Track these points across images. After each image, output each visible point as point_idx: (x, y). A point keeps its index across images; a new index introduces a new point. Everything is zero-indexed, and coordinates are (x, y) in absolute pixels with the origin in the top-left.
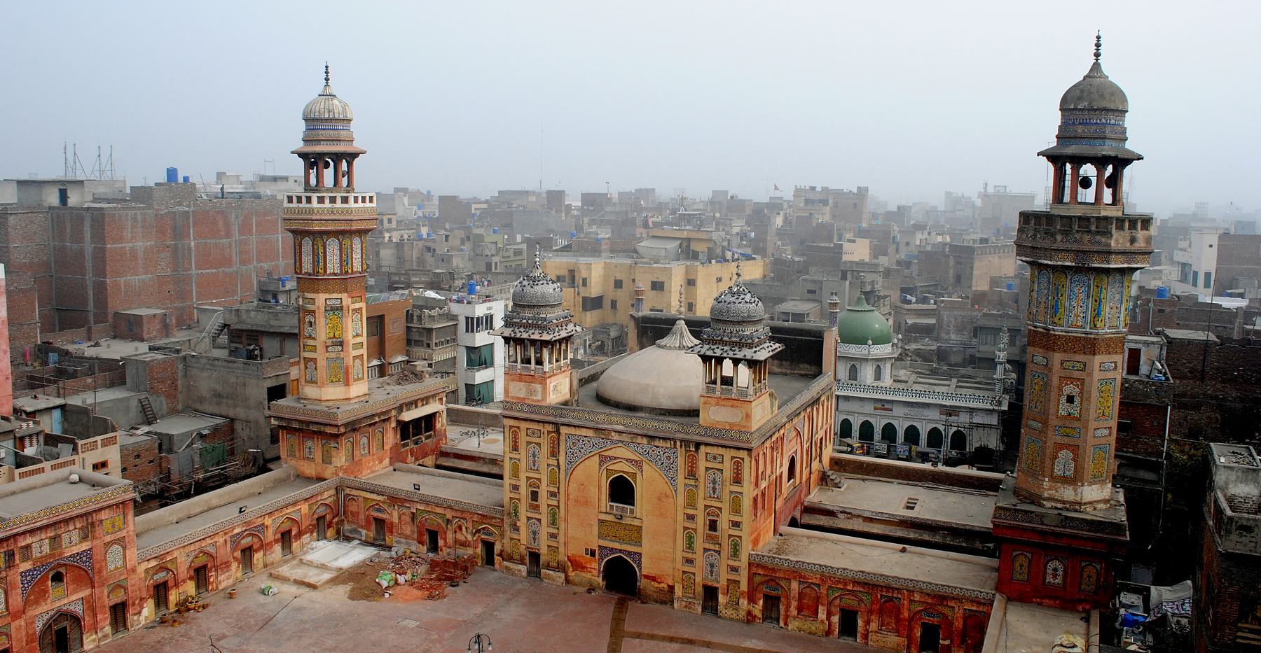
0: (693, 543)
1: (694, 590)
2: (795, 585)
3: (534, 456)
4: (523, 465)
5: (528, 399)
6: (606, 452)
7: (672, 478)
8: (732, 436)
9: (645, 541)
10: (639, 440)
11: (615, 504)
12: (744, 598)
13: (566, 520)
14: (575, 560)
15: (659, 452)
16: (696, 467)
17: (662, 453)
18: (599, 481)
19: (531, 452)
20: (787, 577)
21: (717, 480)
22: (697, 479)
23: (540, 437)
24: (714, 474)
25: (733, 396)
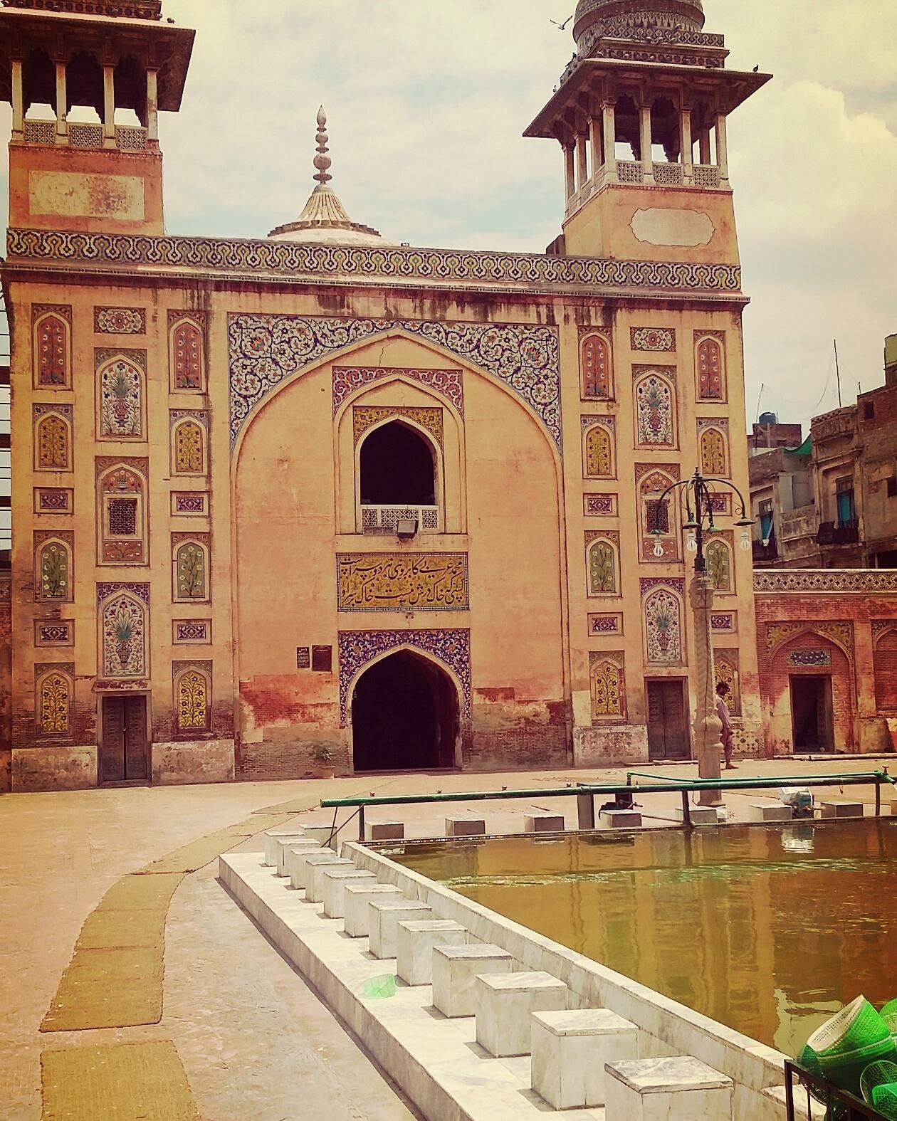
0: (610, 571)
1: (623, 700)
2: (863, 635)
3: (120, 390)
4: (84, 419)
5: (101, 219)
6: (356, 356)
7: (546, 405)
8: (692, 279)
9: (476, 598)
10: (453, 312)
11: (379, 507)
12: (752, 691)
13: (234, 573)
14: (266, 693)
15: (507, 340)
16: (606, 370)
17: (514, 342)
18: (336, 444)
19: (111, 382)
20: (844, 617)
21: (661, 396)
22: (613, 400)
23: (142, 331)
24: (653, 382)
25: (686, 182)
